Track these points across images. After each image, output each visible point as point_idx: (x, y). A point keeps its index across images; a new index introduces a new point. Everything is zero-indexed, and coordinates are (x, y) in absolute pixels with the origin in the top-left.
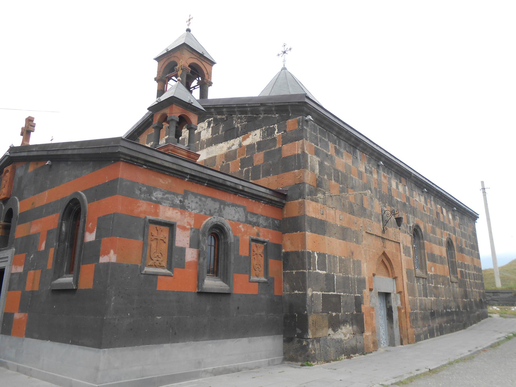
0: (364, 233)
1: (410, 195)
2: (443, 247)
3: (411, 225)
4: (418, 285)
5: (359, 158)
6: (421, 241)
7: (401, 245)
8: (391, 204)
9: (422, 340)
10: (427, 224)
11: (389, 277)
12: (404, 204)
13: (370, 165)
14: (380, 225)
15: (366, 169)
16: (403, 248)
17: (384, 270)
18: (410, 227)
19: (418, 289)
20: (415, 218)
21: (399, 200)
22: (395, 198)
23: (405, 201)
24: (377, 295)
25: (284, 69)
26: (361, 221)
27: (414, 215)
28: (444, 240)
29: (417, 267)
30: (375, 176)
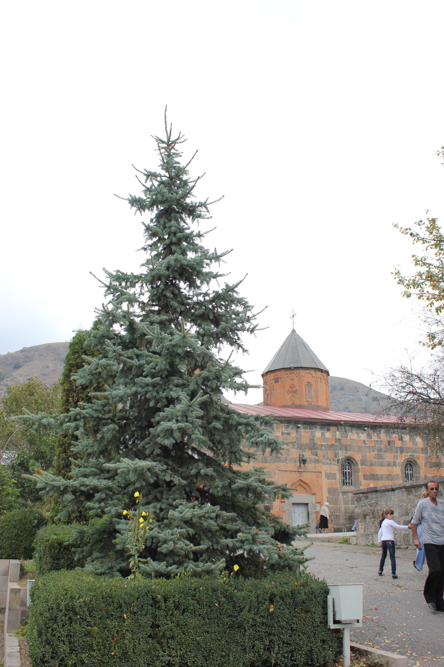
0: (277, 471)
1: (342, 437)
2: (396, 467)
3: (340, 458)
4: (343, 498)
5: (275, 428)
6: (356, 467)
7: (323, 474)
8: (311, 449)
9: (344, 532)
10: (368, 454)
11: (308, 493)
12: (333, 445)
13: (289, 429)
14: (296, 465)
15: (282, 433)
16: (326, 475)
17: (304, 490)
18: (338, 460)
19: (343, 500)
20: (348, 452)
21: (324, 444)
22: (319, 443)
23: (334, 442)
24: (291, 504)
25: (294, 331)
26: (274, 465)
27: (346, 449)
28: (401, 459)
29: (352, 485)
30: (294, 434)
